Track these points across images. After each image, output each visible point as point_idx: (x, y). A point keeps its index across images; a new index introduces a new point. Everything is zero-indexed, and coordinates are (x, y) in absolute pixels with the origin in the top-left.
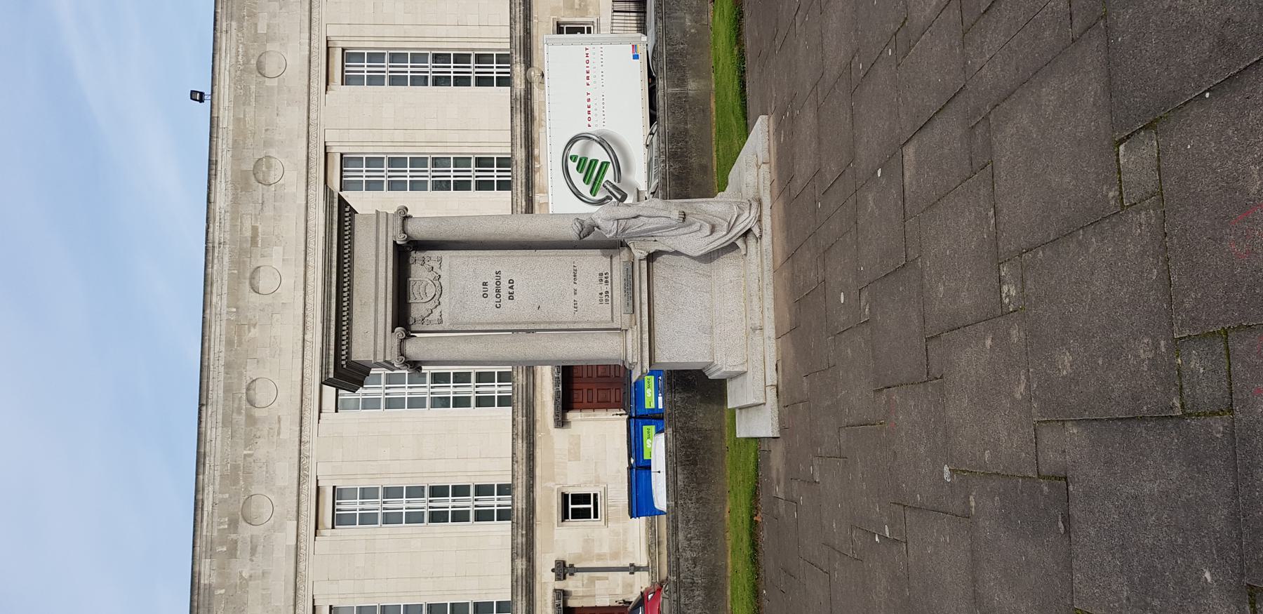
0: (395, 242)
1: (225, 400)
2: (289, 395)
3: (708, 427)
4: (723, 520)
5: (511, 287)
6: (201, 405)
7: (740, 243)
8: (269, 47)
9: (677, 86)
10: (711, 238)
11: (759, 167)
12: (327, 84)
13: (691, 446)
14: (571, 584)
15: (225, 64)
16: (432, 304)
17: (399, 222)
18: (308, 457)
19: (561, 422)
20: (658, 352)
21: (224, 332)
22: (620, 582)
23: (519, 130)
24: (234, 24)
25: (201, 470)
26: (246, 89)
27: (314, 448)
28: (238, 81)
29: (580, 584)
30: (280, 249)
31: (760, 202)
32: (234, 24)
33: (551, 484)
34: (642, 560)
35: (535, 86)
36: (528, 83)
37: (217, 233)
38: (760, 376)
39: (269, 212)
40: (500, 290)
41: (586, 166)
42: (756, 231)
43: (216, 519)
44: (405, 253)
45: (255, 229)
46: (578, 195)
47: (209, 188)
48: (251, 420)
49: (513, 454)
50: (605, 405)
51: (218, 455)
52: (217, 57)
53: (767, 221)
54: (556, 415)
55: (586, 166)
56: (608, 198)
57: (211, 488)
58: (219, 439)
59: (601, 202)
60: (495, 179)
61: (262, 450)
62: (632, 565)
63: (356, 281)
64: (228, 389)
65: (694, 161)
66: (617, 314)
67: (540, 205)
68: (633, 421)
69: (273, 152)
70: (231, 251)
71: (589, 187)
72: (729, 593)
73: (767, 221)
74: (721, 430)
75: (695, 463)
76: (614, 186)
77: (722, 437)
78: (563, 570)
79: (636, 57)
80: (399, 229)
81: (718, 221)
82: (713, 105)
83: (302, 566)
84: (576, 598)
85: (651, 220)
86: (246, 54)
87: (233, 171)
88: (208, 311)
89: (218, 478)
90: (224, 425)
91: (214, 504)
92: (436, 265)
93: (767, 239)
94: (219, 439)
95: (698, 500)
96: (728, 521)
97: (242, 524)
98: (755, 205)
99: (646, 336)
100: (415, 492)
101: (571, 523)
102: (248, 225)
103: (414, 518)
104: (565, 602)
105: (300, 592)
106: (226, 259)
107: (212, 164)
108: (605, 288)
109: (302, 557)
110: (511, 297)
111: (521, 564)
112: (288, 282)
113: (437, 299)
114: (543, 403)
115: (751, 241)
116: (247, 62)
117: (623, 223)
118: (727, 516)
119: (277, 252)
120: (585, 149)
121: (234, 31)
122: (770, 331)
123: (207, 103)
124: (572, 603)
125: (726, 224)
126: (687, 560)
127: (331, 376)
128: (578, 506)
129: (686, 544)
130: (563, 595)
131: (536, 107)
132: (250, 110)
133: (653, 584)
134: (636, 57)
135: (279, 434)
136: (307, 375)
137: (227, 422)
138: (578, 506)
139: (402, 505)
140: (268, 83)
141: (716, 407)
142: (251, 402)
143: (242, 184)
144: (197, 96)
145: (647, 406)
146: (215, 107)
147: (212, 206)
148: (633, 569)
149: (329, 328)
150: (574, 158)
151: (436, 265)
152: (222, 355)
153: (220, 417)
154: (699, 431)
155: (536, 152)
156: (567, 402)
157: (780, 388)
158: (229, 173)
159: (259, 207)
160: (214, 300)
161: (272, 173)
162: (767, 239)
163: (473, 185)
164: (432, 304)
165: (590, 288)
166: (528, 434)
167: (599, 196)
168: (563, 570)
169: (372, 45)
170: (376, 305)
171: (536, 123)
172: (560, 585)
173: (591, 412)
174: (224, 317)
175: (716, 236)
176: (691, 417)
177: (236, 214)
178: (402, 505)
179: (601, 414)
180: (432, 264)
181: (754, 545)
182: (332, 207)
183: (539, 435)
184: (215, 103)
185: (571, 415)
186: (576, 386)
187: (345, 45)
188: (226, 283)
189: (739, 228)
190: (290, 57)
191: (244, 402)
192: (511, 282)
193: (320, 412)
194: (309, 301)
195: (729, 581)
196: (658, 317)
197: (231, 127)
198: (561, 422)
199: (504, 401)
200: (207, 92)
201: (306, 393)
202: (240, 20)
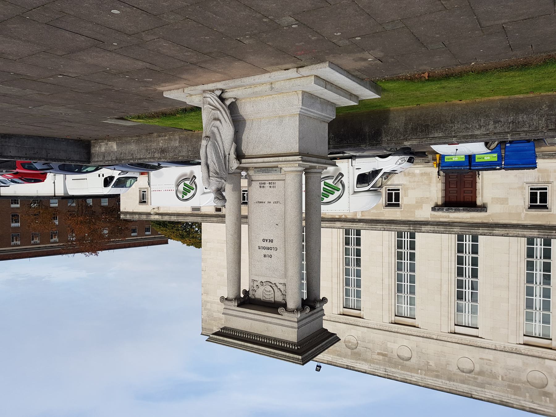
1: (468, 384)
2: (467, 351)
3: (404, 119)
4: (467, 104)
6: (471, 397)
7: (228, 103)
10: (222, 120)
13: (417, 129)
16: (275, 288)
17: (227, 302)
18: (505, 347)
19: (483, 208)
20: (293, 151)
21: (431, 378)
25: (511, 405)
27: (500, 344)
30: (389, 344)
31: (204, 91)
33: (523, 215)
37: (381, 372)
38: (298, 81)
39: (370, 346)
42: (218, 93)
43: (543, 403)
45: (379, 354)
46: (339, 197)
48: (481, 373)
49: (502, 236)
50: (473, 184)
51: (502, 394)
53: (211, 86)
54: (477, 211)
56: (341, 182)
57: (523, 402)
58: (492, 392)
59: (343, 186)
61: (499, 370)
64: (463, 382)
67: (362, 216)
68: (472, 168)
70: (389, 367)
71: (336, 192)
72: (521, 96)
73: (211, 86)
74: (406, 111)
75: (427, 126)
77: (410, 109)
85: (209, 156)
87: (351, 359)
88: (420, 384)
89: (516, 397)
90: (484, 388)
91: (532, 402)
92: (256, 283)
93: (220, 85)
94: (492, 392)
95: (452, 122)
96: (468, 101)
97: (546, 389)
100: (530, 292)
101: (549, 204)
102: (376, 357)
103: (547, 294)
106: (393, 370)
107: (348, 368)
108: (267, 185)
110: (271, 241)
112: (405, 343)
114: (471, 218)
115: (225, 95)
117: (211, 174)
118: (463, 102)
119: (390, 345)
122: (264, 78)
123: (321, 364)
125: (213, 111)
126: (495, 127)
127: (300, 357)
128: (538, 199)
129: (483, 129)
135: (490, 360)
136: (456, 341)
137: (482, 385)
138: (538, 199)
139: (538, 299)
141: (392, 115)
142: (471, 372)
143: (357, 356)
144: (318, 368)
145: (464, 160)
147: (368, 372)
149: (274, 354)
151: (256, 283)
152: (444, 381)
153: (479, 389)
154: (406, 124)
155: (337, 217)
156: (471, 205)
157: (296, 65)
158: (352, 361)
159: (368, 350)
160: (415, 380)
161: (352, 341)
162: (220, 85)
163: (358, 247)
164: (275, 288)
166: (491, 227)
173: (477, 191)
174: (423, 376)
175: (221, 117)
176: (398, 130)
178: (538, 299)
179: (479, 186)
180: (255, 286)
181: (447, 77)
182: (216, 339)
183: (491, 221)
184: (321, 361)
185: (479, 202)
186: (462, 200)
188: (405, 373)
189: (217, 103)
191: (470, 375)
193: (478, 337)
194: (415, 334)
195: (512, 97)
196: (274, 151)
197: (332, 356)
198: (483, 208)
199: (475, 239)
200: (316, 363)
201: (466, 342)
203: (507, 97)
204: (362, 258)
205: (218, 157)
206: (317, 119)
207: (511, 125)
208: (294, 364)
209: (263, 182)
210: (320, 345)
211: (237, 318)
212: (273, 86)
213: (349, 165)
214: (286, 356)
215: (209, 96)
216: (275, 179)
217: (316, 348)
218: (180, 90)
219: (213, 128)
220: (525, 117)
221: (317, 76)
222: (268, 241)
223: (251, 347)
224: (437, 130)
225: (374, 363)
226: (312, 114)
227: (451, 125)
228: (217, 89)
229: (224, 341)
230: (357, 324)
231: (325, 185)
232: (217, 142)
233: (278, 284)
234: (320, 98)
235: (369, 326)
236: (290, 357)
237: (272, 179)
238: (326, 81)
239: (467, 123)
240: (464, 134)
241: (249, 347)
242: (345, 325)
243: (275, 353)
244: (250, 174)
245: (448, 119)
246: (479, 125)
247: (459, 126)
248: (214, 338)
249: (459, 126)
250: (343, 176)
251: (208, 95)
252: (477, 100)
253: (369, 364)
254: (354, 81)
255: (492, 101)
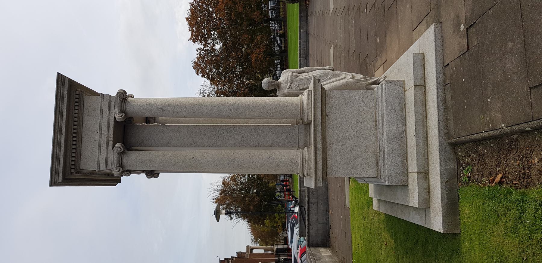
206: (377, 141)
210: (64, 130)
217: (64, 118)
221: (424, 58)
226: (380, 118)
232: (330, 79)
234: (406, 131)
238: (424, 86)
254: (438, 106)
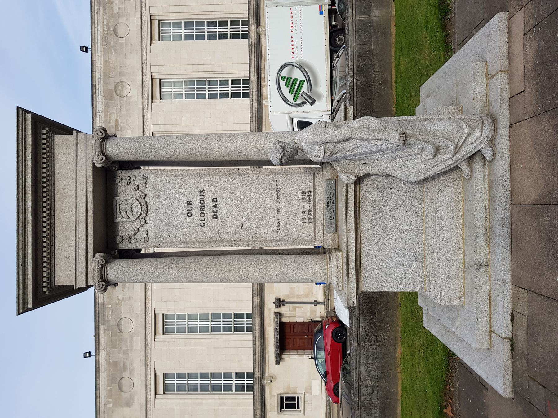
0: (94, 164)
4: (395, 358)
5: (215, 206)
7: (464, 166)
8: (120, 20)
9: (364, 13)
10: (433, 163)
11: (490, 77)
12: (151, 40)
14: (283, 310)
15: (98, 30)
17: (97, 143)
20: (364, 280)
22: (309, 310)
23: (253, 63)
24: (101, 8)
26: (109, 44)
28: (105, 40)
29: (288, 310)
32: (101, 8)
34: (321, 299)
35: (262, 37)
36: (258, 35)
37: (98, 124)
39: (124, 112)
40: (204, 209)
41: (291, 83)
44: (108, 175)
45: (117, 121)
46: (286, 101)
47: (93, 99)
52: (93, 27)
55: (291, 83)
56: (304, 102)
59: (300, 105)
60: (242, 92)
62: (315, 301)
63: (57, 204)
65: (377, 75)
66: (320, 231)
69: (124, 79)
71: (292, 96)
73: (503, 143)
75: (373, 314)
76: (307, 95)
78: (279, 302)
79: (321, 13)
80: (97, 150)
81: (443, 142)
82: (393, 29)
83: (148, 294)
84: (286, 317)
85: (365, 143)
86: (108, 25)
92: (142, 184)
93: (502, 166)
95: (375, 343)
98: (488, 122)
99: (353, 266)
102: (113, 119)
104: (280, 319)
105: (148, 307)
107: (93, 86)
108: (307, 206)
109: (148, 290)
110: (215, 216)
111: (257, 299)
113: (143, 218)
115: (478, 164)
116: (109, 29)
120: (290, 72)
121: (101, 12)
124: (284, 320)
125: (453, 147)
129: (366, 375)
130: (279, 315)
131: (263, 49)
132: (112, 56)
133: (327, 312)
134: (321, 13)
140: (120, 40)
143: (110, 96)
144: (84, 49)
146: (94, 55)
148: (316, 303)
150: (283, 78)
151: (142, 184)
155: (263, 75)
158: (102, 91)
159: (118, 109)
165: (292, 206)
167: (299, 102)
168: (279, 302)
169: (174, 17)
170: (77, 229)
171: (263, 59)
172: (277, 310)
175: (439, 159)
177: (107, 114)
180: (138, 182)
184: (93, 52)
187: (160, 18)
189: (466, 151)
190: (131, 26)
192: (215, 200)
196: (366, 244)
197: (102, 66)
200: (89, 47)
202: (104, 6)
203: (399, 398)
204: (219, 100)
205: (362, 154)
207: (368, 402)
208: (15, 300)
209: (312, 198)
211: (73, 162)
212: (483, 268)
213: (324, 111)
214: (26, 279)
215: (484, 135)
216: (317, 219)
218: (505, 62)
219: (421, 147)
220: (376, 415)
222: (215, 209)
223: (26, 209)
224: (368, 326)
225: (106, 116)
227: (373, 341)
228: (494, 152)
229: (26, 148)
230: (145, 96)
231: (301, 81)
233: (145, 227)
235: (145, 111)
236: (26, 288)
237: (317, 214)
239: (374, 358)
240: (361, 355)
241: (26, 204)
242: (141, 82)
243: (26, 257)
244: (325, 171)
245: (380, 338)
246: (371, 371)
247: (371, 350)
248: (26, 125)
249: (371, 350)
250: (312, 104)
251: (486, 130)
252: (399, 369)
253: (103, 110)
255: (396, 384)
